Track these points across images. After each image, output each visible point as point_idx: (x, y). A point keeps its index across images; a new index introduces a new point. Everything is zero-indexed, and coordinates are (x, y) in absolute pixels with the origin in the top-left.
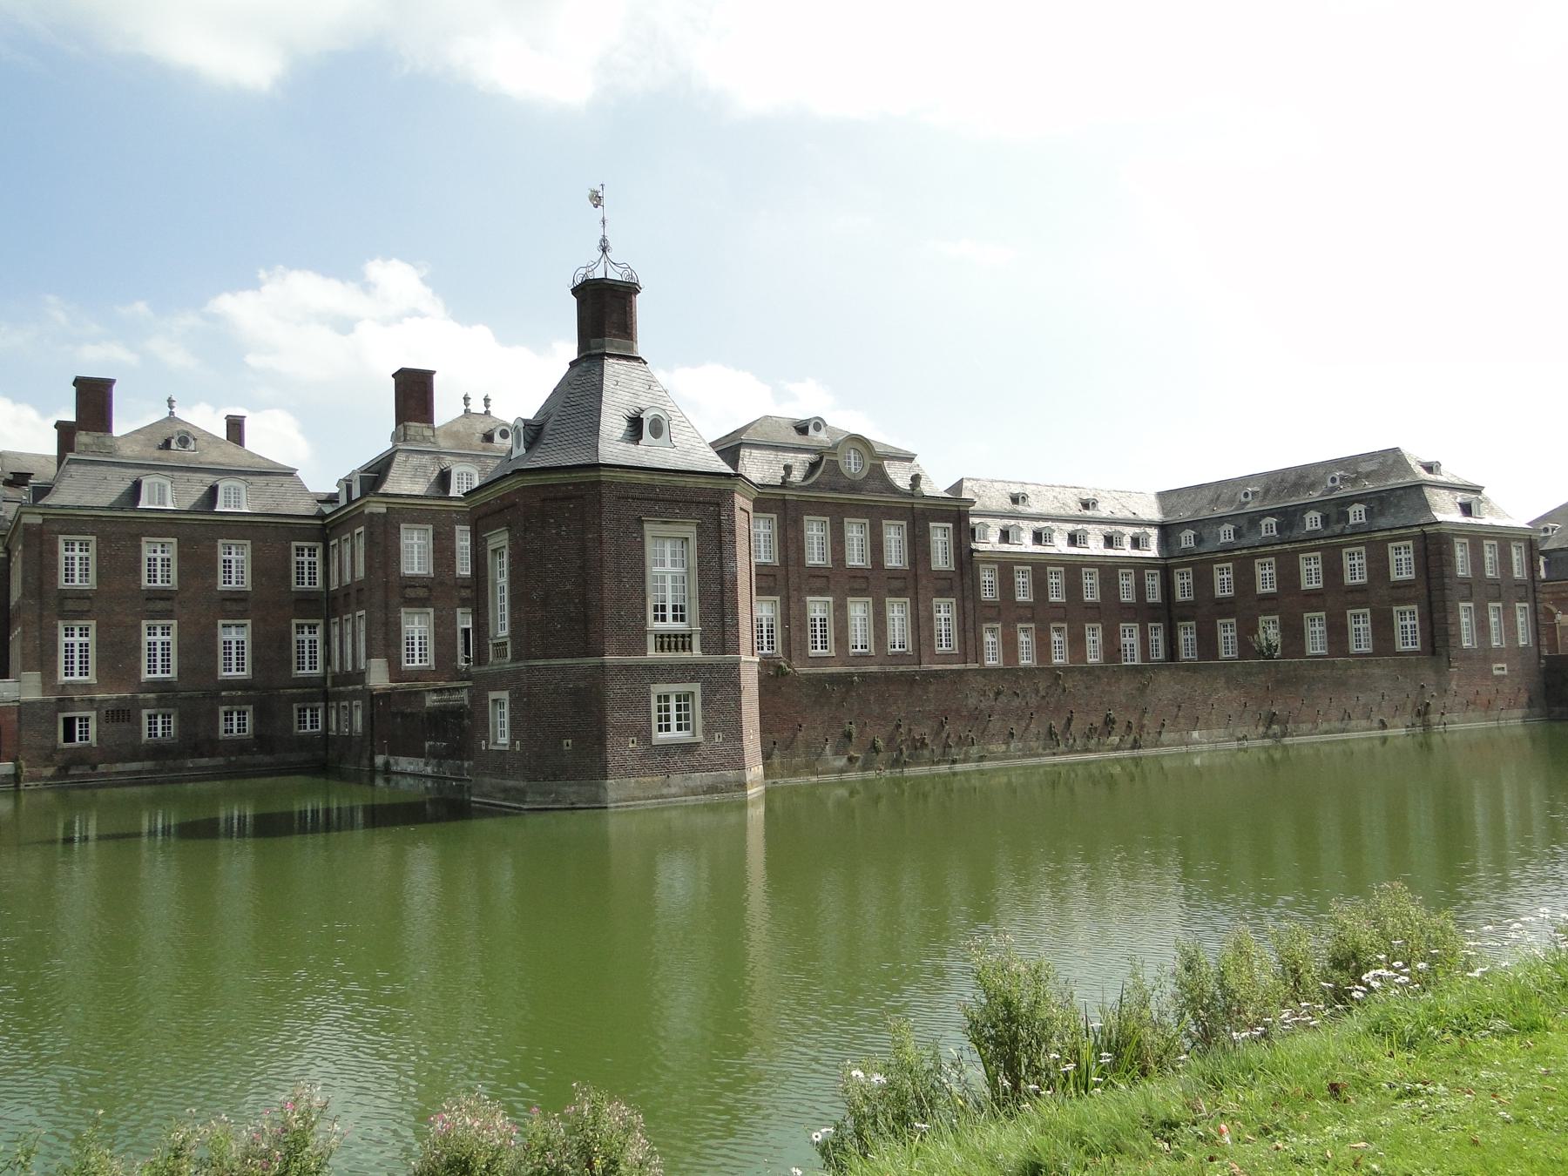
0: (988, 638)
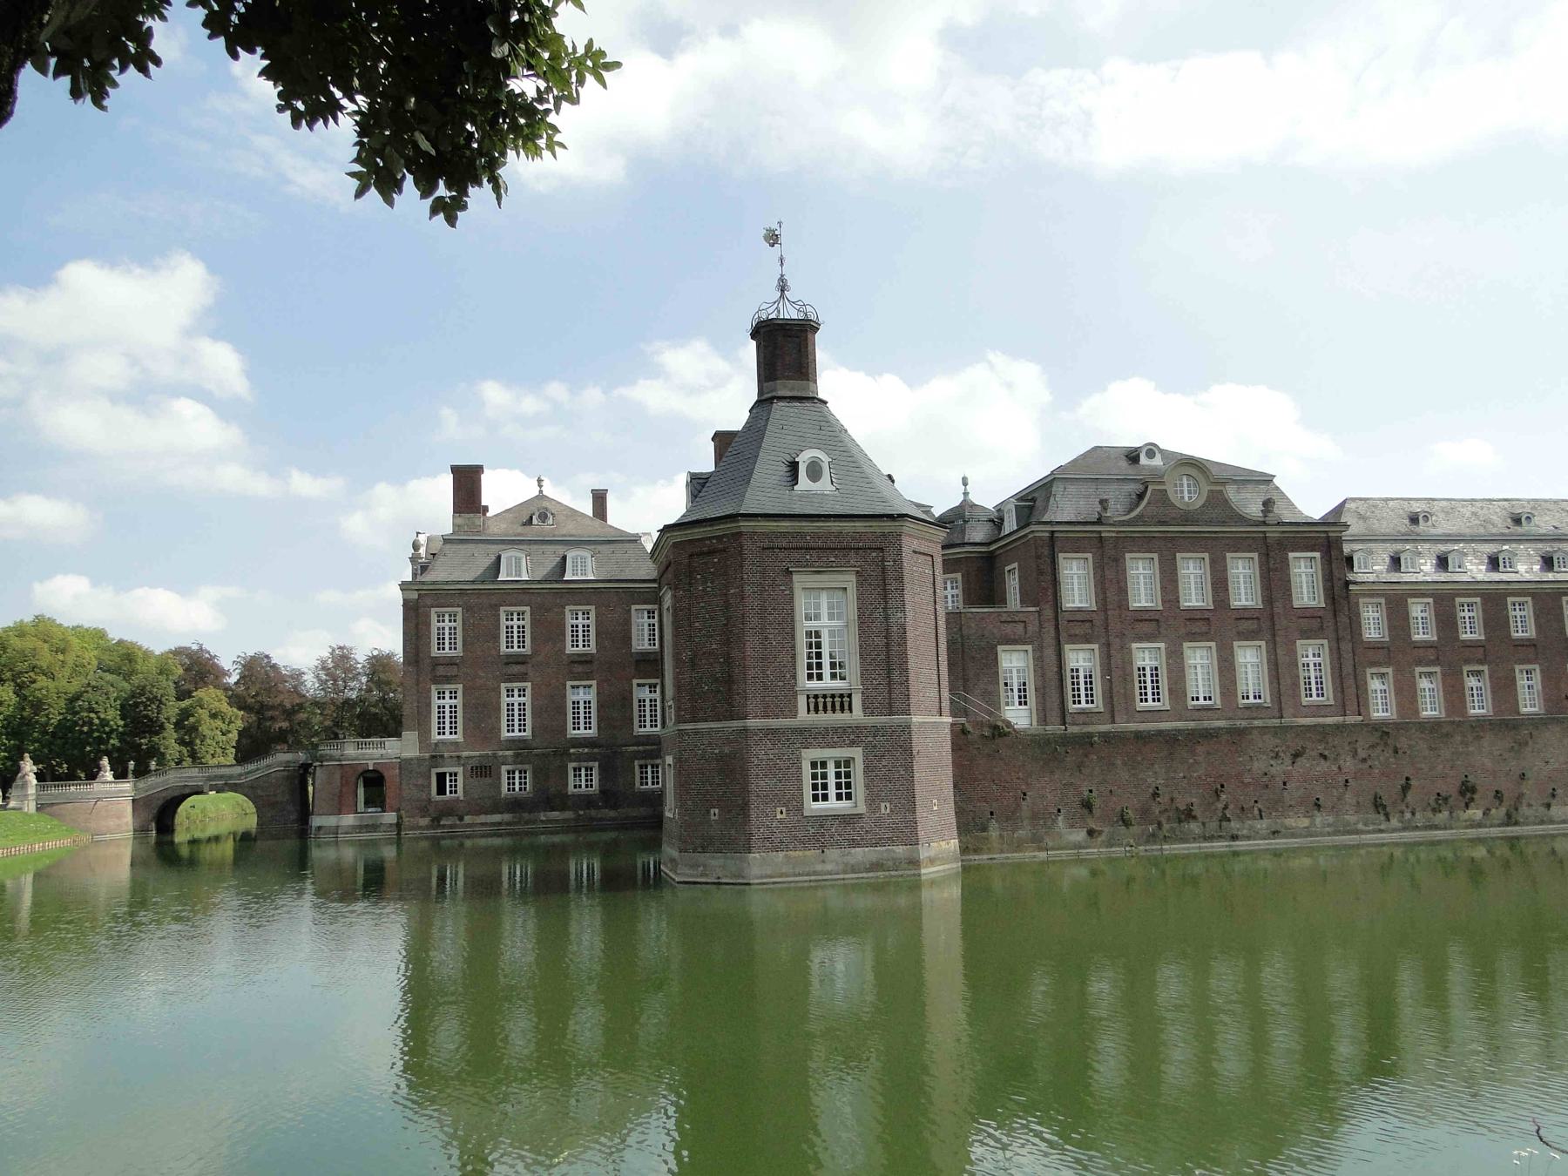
0: (1375, 685)
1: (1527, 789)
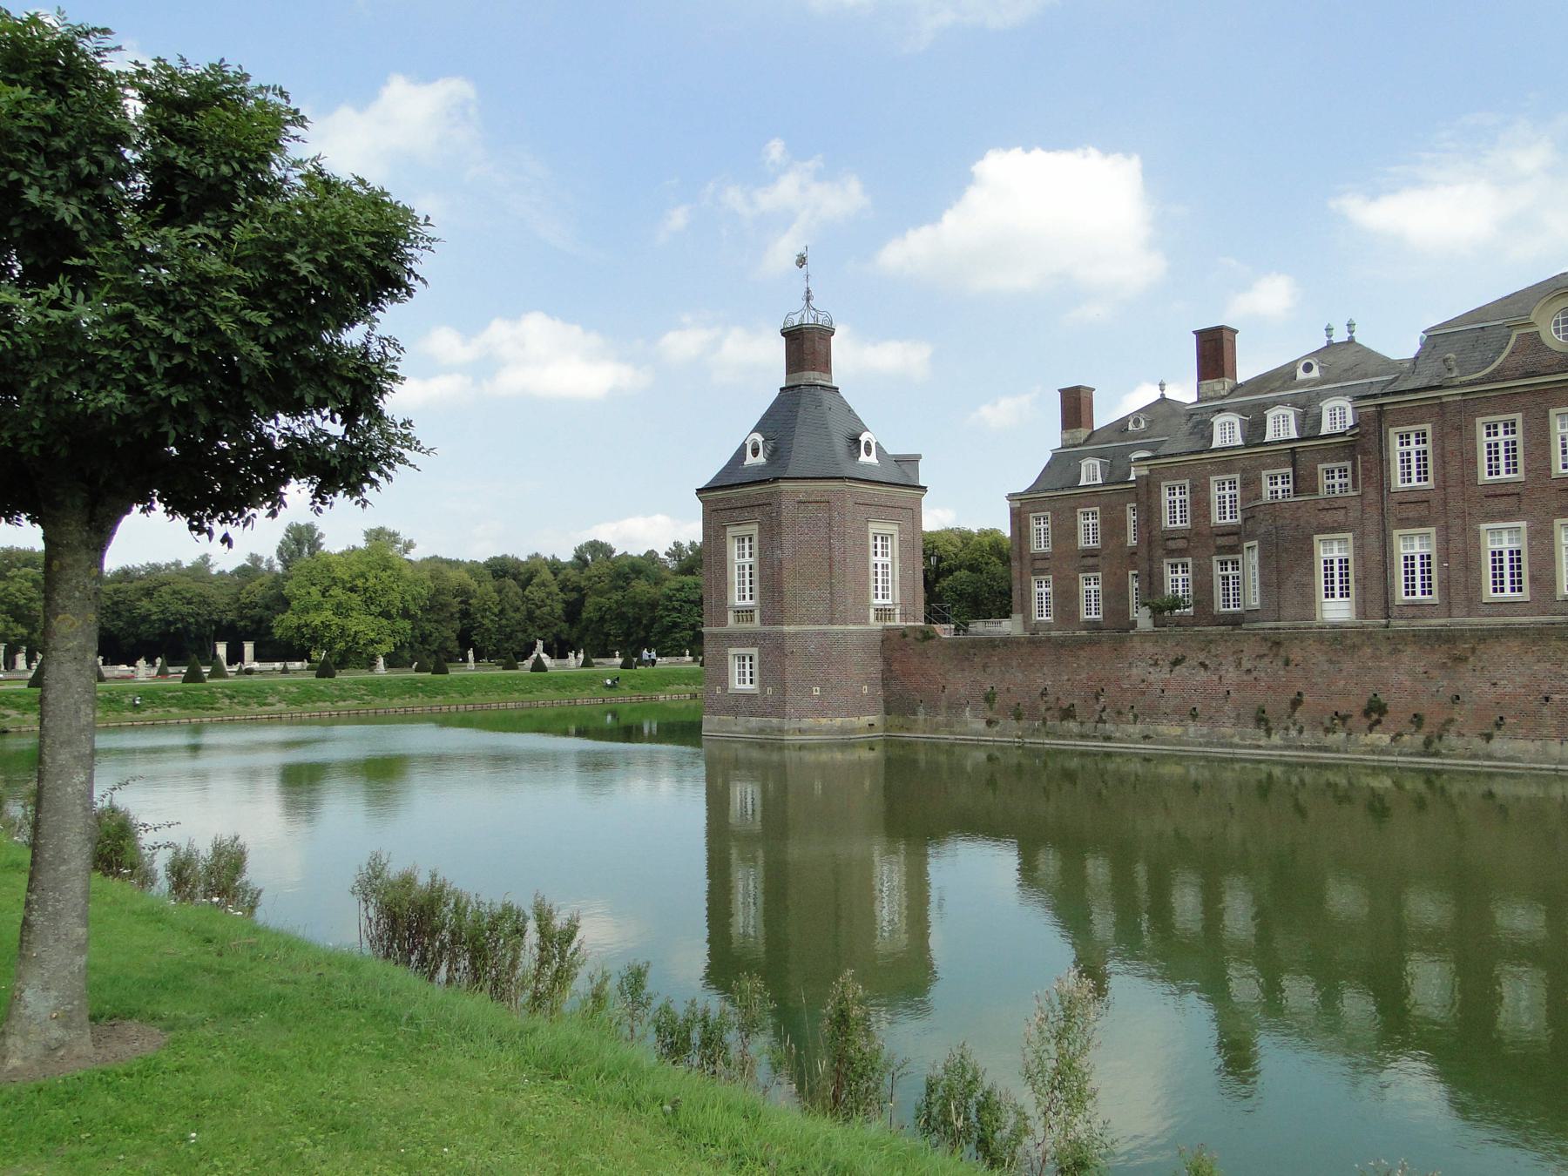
1: (1459, 714)
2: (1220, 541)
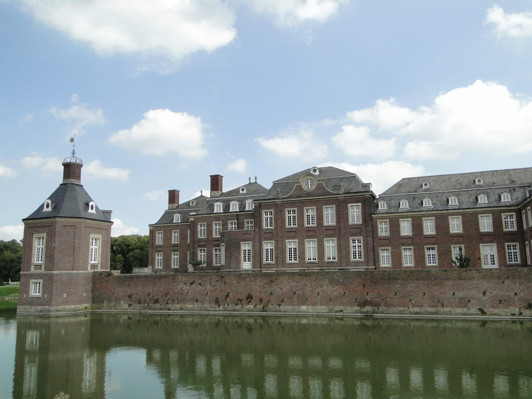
1: (272, 298)
2: (215, 243)
